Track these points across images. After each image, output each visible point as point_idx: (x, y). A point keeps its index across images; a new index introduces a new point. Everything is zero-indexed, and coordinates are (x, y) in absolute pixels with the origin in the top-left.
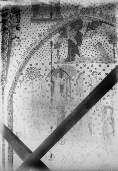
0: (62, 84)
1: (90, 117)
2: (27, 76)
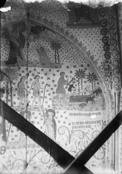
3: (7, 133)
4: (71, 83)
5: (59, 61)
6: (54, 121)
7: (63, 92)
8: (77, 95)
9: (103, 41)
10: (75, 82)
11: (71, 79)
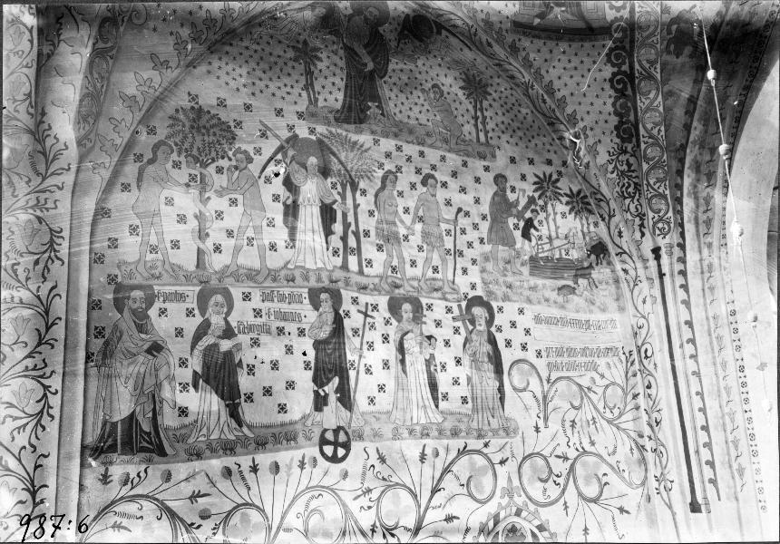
0: (327, 201)
1: (430, 338)
2: (176, 144)
3: (352, 374)
4: (528, 215)
5: (486, 136)
6: (492, 341)
7: (510, 243)
8: (546, 254)
9: (612, 87)
10: (537, 211)
11: (526, 200)
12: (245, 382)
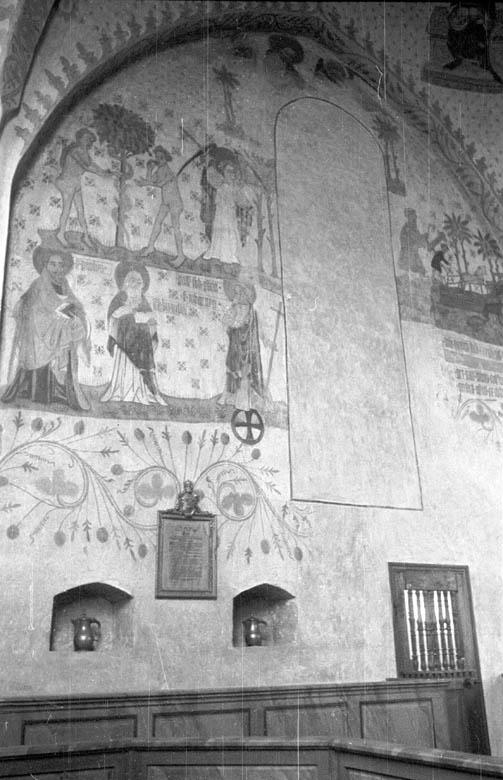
4: (438, 248)
12: (159, 356)
